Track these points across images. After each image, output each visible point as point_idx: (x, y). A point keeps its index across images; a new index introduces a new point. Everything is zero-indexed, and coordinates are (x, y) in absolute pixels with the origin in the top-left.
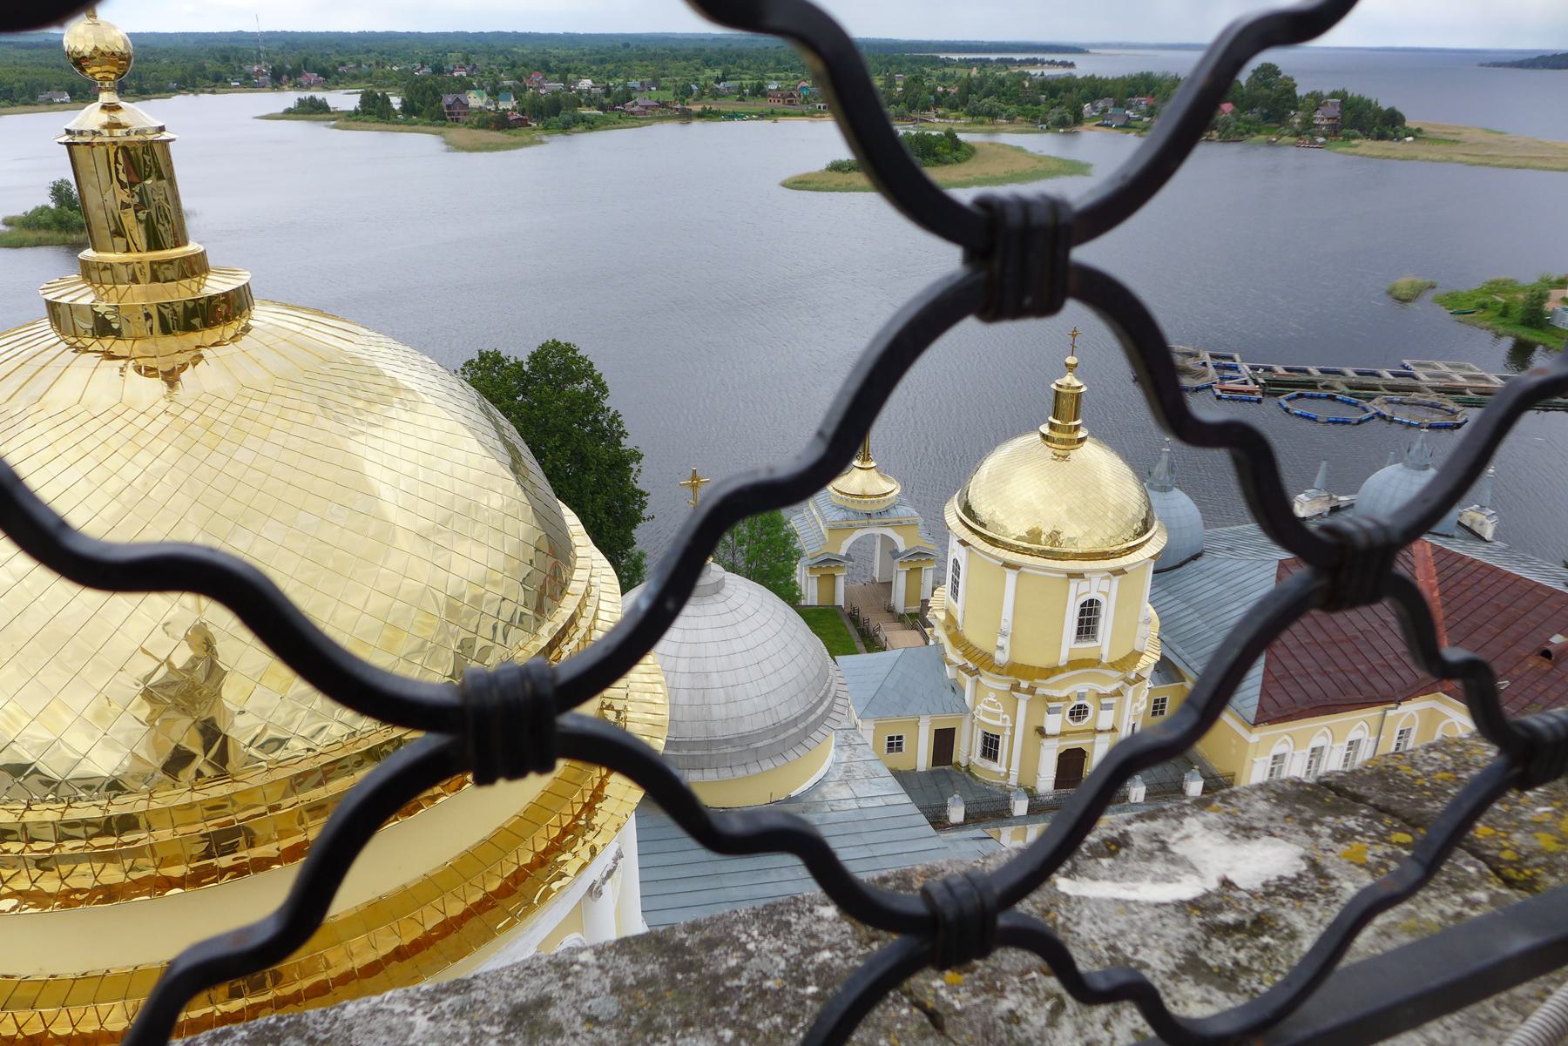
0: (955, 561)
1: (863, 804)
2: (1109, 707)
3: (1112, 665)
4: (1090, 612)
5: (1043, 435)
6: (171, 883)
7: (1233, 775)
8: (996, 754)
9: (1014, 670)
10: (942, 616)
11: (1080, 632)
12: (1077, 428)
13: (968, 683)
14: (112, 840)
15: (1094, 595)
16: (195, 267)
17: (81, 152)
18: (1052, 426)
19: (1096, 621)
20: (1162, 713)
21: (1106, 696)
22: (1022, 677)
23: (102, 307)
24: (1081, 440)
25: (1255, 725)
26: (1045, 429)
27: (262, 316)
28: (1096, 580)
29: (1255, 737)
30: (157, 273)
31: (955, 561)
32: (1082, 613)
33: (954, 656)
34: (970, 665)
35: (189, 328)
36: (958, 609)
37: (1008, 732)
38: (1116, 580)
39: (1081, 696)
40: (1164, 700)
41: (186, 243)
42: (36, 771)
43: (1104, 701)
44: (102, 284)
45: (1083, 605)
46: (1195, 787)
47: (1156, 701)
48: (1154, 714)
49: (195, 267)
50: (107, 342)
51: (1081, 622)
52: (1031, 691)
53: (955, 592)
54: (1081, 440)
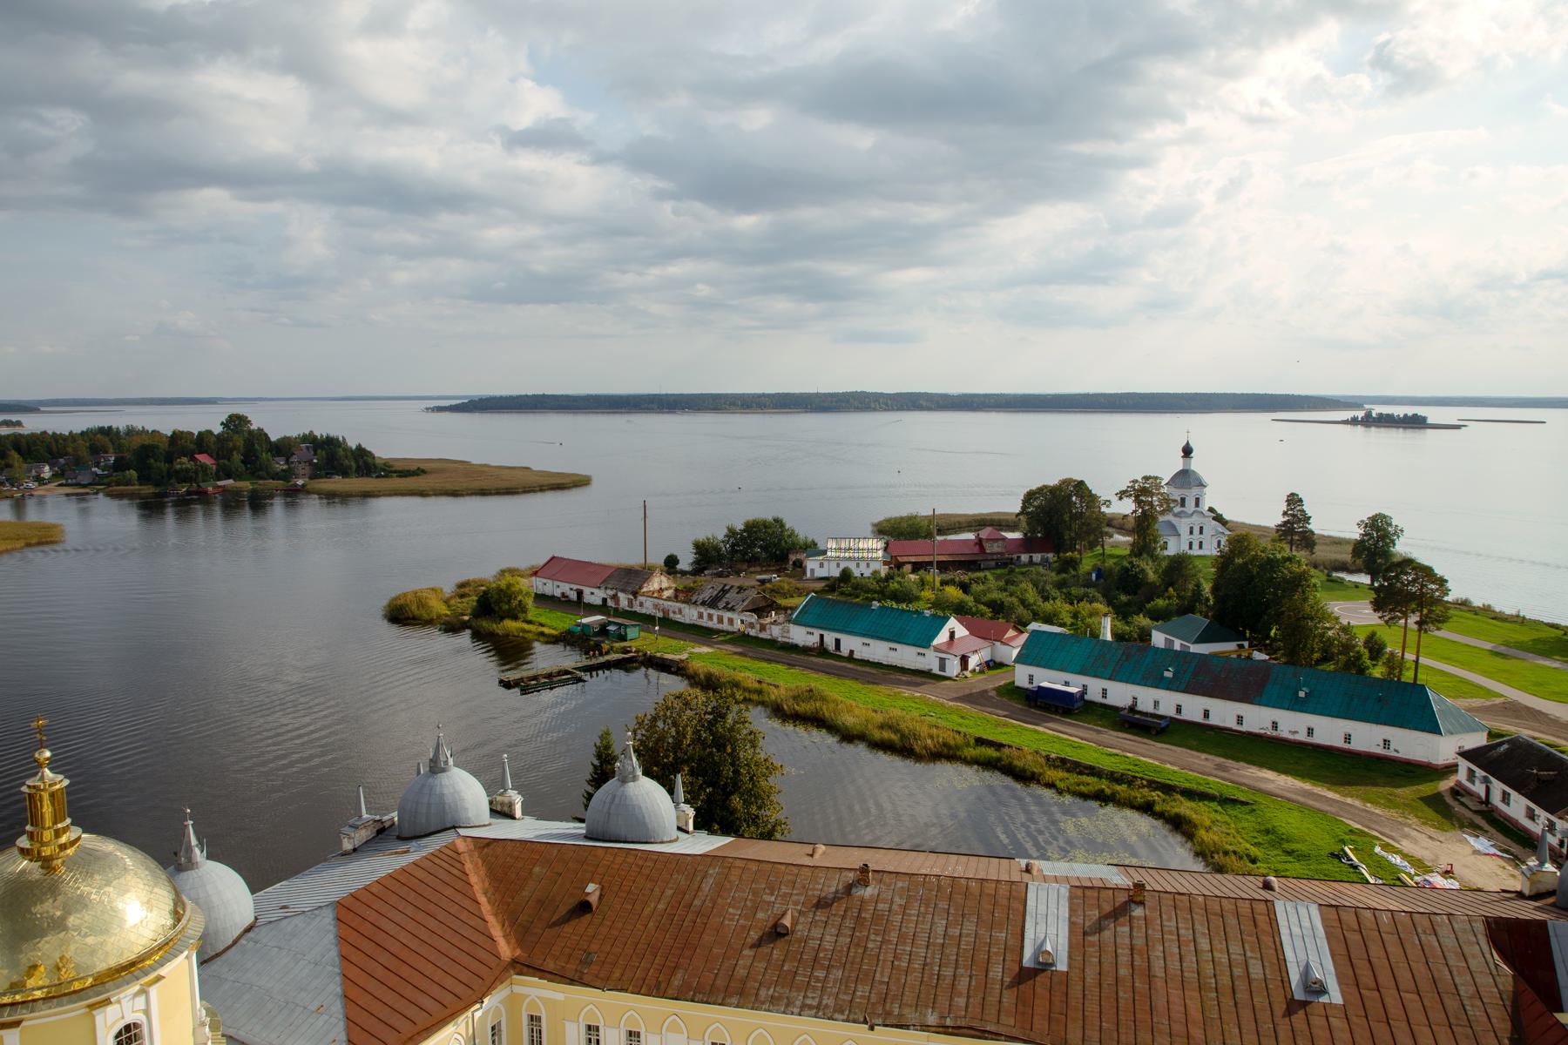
12: (65, 830)
15: (129, 1020)
18: (31, 837)
38: (154, 991)
45: (119, 1034)
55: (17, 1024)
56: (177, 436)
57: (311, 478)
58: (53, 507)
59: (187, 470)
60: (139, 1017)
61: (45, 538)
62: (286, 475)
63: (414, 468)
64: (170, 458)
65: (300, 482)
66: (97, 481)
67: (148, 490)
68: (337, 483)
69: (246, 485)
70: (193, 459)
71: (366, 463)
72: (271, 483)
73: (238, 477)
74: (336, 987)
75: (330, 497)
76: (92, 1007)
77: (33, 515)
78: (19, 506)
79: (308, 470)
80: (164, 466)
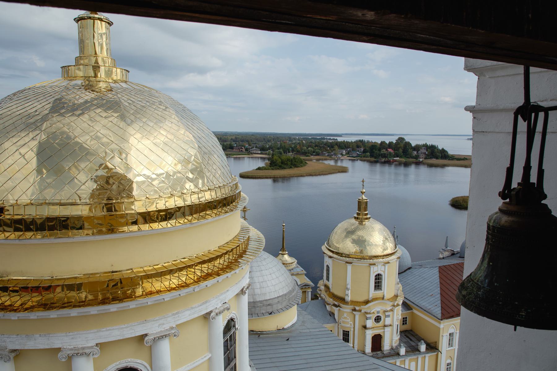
0: (328, 266)
1: (311, 330)
2: (389, 316)
3: (388, 300)
4: (379, 279)
5: (355, 218)
7: (436, 343)
8: (348, 339)
9: (353, 302)
10: (323, 288)
11: (375, 286)
12: (366, 214)
13: (336, 310)
15: (379, 272)
18: (358, 214)
19: (381, 282)
20: (406, 323)
21: (387, 311)
22: (356, 306)
24: (370, 218)
25: (442, 320)
26: (356, 215)
28: (379, 266)
29: (442, 326)
31: (328, 266)
32: (376, 279)
33: (330, 301)
34: (336, 303)
36: (330, 284)
37: (352, 329)
38: (387, 265)
39: (378, 312)
40: (406, 318)
43: (387, 314)
45: (376, 276)
46: (423, 348)
47: (404, 318)
48: (403, 324)
51: (375, 283)
52: (360, 311)
53: (328, 279)
54: (370, 218)
55: (351, 263)
56: (383, 143)
57: (425, 158)
58: (346, 163)
59: (385, 154)
60: (382, 273)
61: (344, 170)
62: (417, 157)
63: (463, 157)
64: (380, 150)
65: (421, 160)
66: (358, 156)
67: (373, 159)
68: (434, 161)
69: (403, 160)
70: (387, 150)
71: (445, 155)
72: (411, 160)
73: (401, 157)
74: (438, 290)
75: (431, 166)
76: (371, 264)
77: (339, 164)
78: (336, 161)
79: (424, 156)
80: (377, 152)
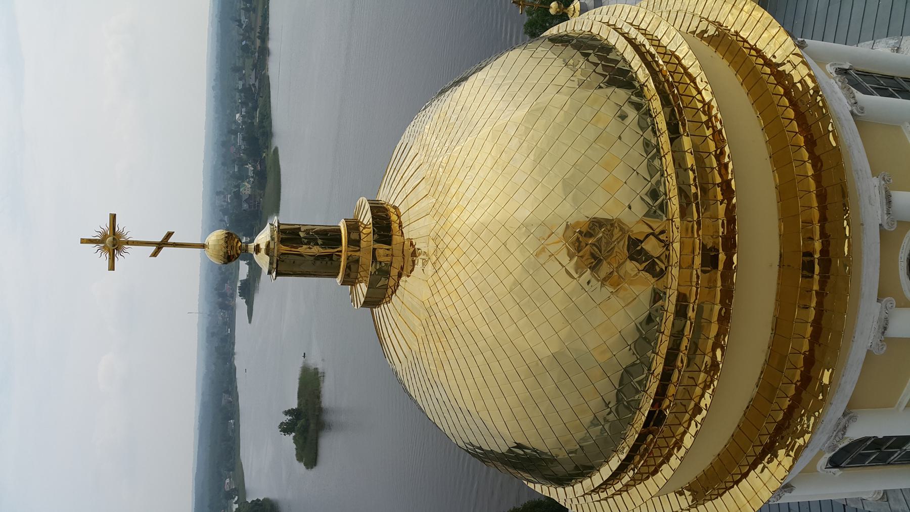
6: (729, 262)
14: (691, 305)
16: (354, 226)
17: (282, 268)
23: (371, 269)
27: (383, 196)
30: (354, 243)
35: (388, 228)
41: (339, 231)
42: (641, 324)
44: (357, 278)
49: (354, 226)
50: (394, 272)
